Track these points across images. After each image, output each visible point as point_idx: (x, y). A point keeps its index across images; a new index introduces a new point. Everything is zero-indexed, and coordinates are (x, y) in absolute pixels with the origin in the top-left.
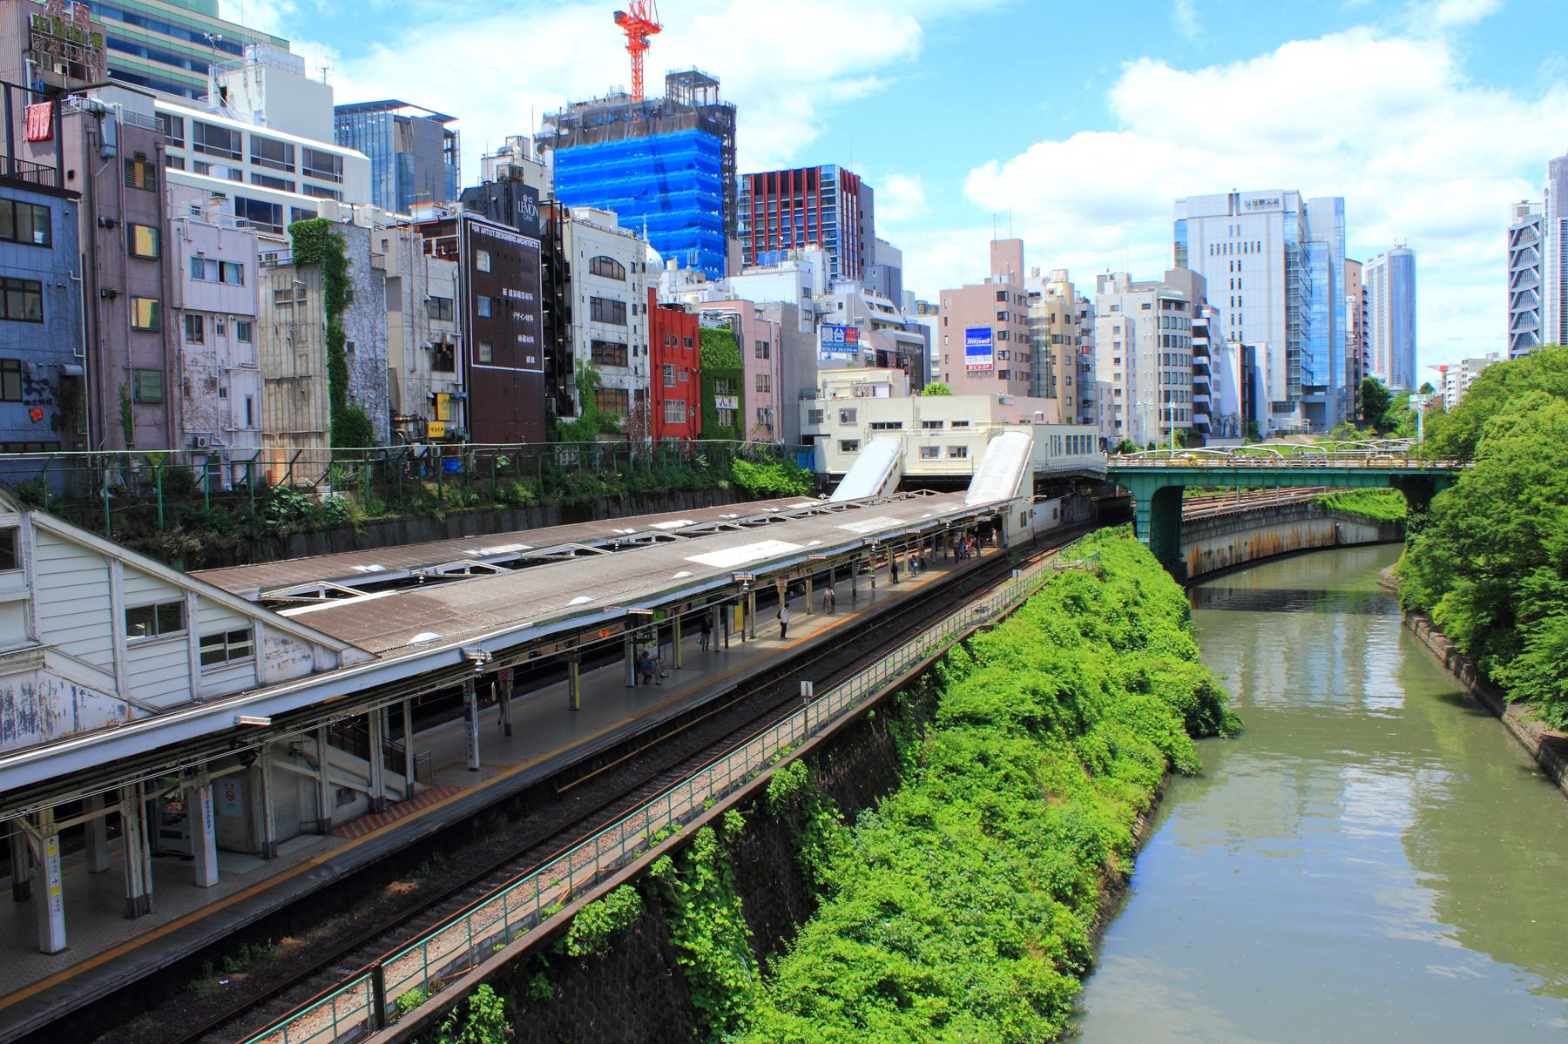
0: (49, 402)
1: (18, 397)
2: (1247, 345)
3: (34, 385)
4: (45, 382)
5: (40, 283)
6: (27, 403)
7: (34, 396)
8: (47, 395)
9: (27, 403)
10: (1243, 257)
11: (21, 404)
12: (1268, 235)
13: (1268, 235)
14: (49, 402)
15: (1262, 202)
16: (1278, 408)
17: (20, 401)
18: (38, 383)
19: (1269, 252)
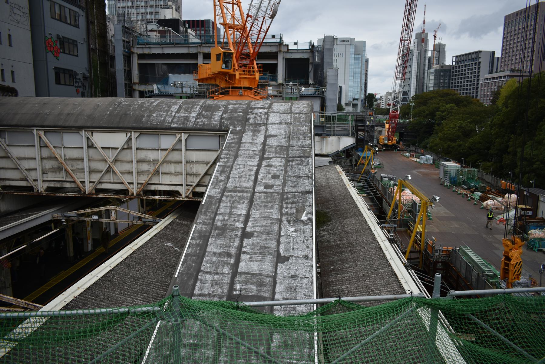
0: (80, 87)
1: (72, 84)
2: (340, 85)
3: (77, 80)
4: (79, 79)
5: (77, 41)
6: (76, 87)
7: (77, 85)
8: (80, 84)
9: (76, 87)
10: (337, 58)
11: (74, 87)
12: (346, 52)
13: (346, 52)
14: (80, 87)
15: (344, 41)
16: (347, 104)
17: (73, 85)
18: (78, 79)
19: (345, 57)
